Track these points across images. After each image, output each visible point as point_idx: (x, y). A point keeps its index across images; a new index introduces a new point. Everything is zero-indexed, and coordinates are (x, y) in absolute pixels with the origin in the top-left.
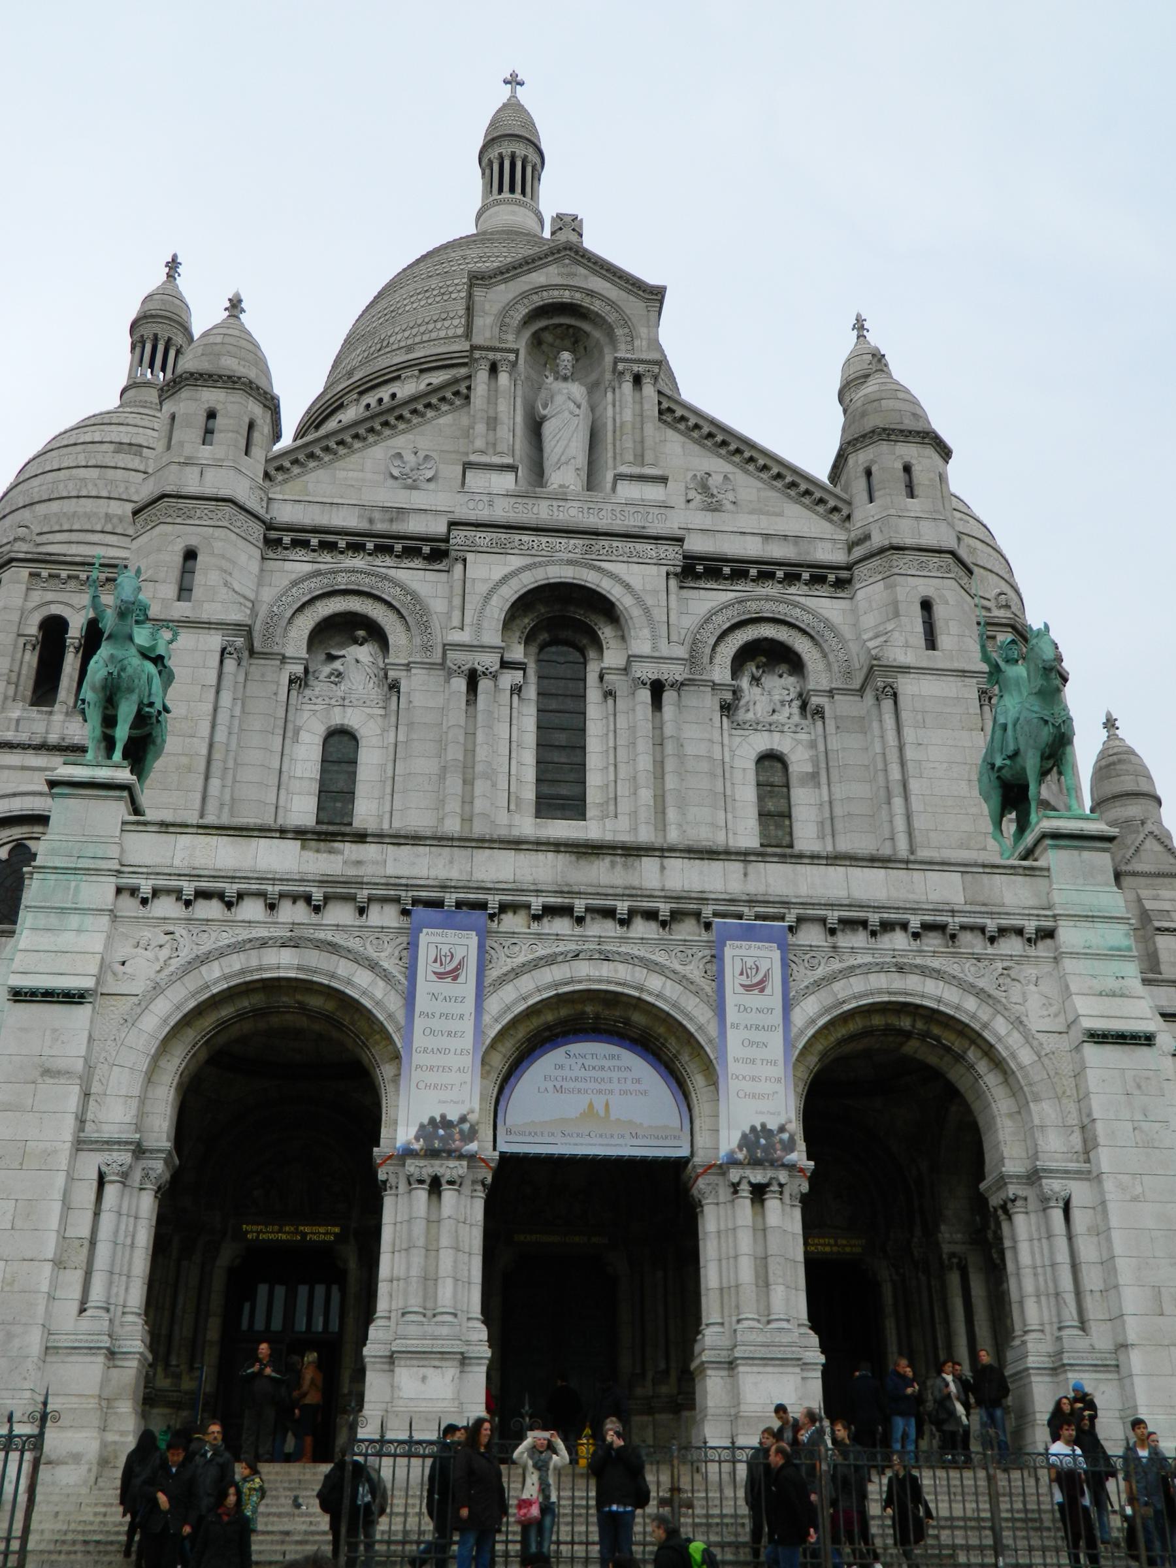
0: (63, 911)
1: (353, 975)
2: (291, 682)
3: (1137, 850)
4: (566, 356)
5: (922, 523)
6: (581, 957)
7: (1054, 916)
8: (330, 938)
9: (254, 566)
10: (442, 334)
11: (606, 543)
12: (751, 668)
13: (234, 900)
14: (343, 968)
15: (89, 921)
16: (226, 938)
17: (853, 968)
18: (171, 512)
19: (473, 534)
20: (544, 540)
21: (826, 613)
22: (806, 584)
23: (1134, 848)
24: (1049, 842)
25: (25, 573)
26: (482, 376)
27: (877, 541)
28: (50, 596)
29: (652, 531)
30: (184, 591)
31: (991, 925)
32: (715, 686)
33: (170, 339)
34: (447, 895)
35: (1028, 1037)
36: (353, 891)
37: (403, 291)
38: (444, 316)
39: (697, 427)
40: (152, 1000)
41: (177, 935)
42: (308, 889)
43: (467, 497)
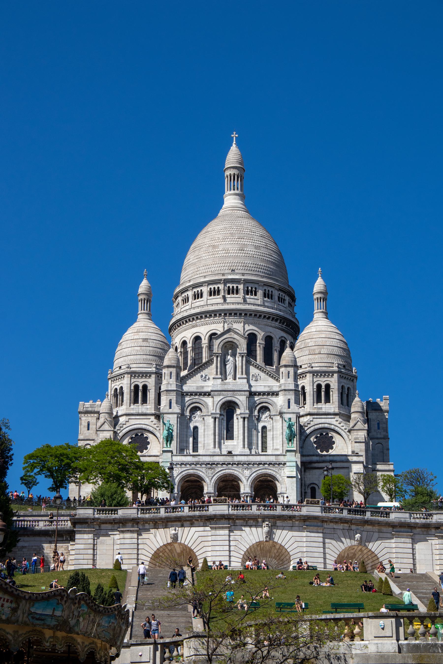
3: (355, 425)
4: (230, 351)
9: (180, 400)
10: (213, 269)
12: (262, 410)
14: (198, 472)
16: (185, 469)
21: (274, 400)
25: (129, 375)
27: (283, 388)
28: (135, 380)
29: (244, 389)
30: (170, 408)
31: (278, 463)
35: (281, 477)
37: (202, 250)
38: (213, 263)
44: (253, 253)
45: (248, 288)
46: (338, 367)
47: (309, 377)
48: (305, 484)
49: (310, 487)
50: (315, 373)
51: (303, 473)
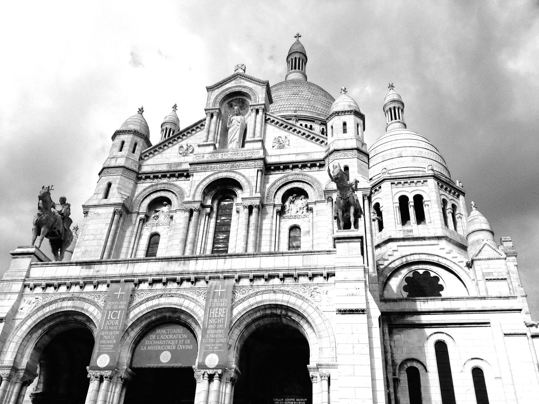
0: (6, 293)
1: (88, 308)
2: (140, 220)
5: (347, 141)
6: (163, 296)
7: (334, 268)
8: (84, 297)
11: (238, 164)
12: (291, 198)
13: (57, 286)
14: (86, 306)
15: (13, 295)
17: (257, 293)
18: (106, 172)
19: (196, 167)
20: (218, 165)
21: (315, 176)
22: (310, 167)
23: (479, 250)
24: (336, 241)
26: (208, 118)
27: (332, 149)
29: (254, 157)
30: (106, 196)
31: (310, 273)
32: (275, 206)
33: (171, 128)
34: (122, 279)
35: (320, 315)
36: (92, 280)
39: (278, 123)
40: (27, 320)
41: (39, 299)
42: (79, 281)
43: (197, 155)
44: (310, 97)
45: (301, 125)
46: (433, 170)
47: (386, 186)
48: (393, 361)
49: (406, 367)
50: (395, 180)
51: (387, 337)
